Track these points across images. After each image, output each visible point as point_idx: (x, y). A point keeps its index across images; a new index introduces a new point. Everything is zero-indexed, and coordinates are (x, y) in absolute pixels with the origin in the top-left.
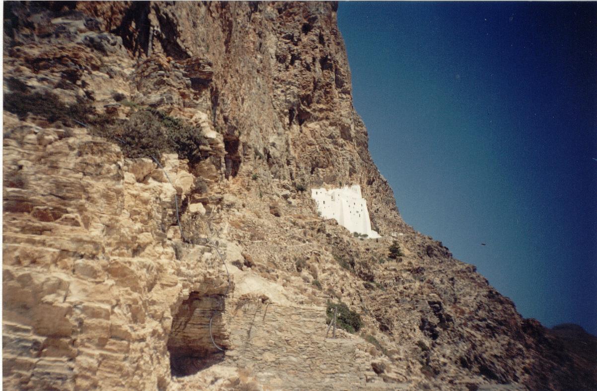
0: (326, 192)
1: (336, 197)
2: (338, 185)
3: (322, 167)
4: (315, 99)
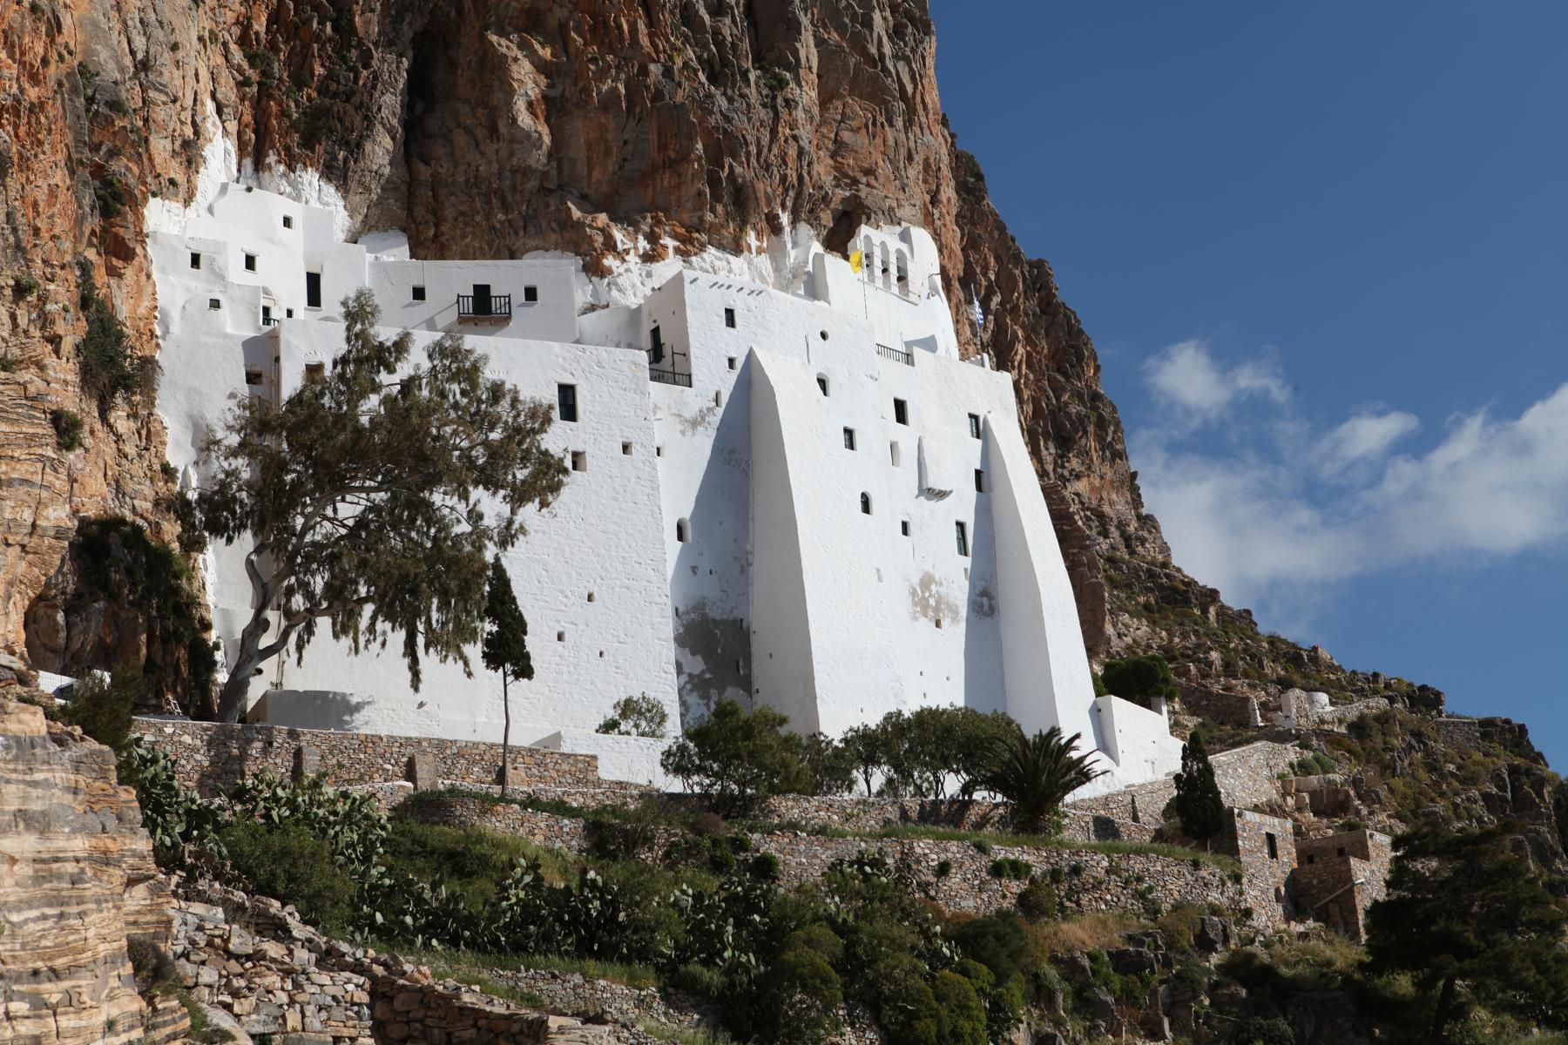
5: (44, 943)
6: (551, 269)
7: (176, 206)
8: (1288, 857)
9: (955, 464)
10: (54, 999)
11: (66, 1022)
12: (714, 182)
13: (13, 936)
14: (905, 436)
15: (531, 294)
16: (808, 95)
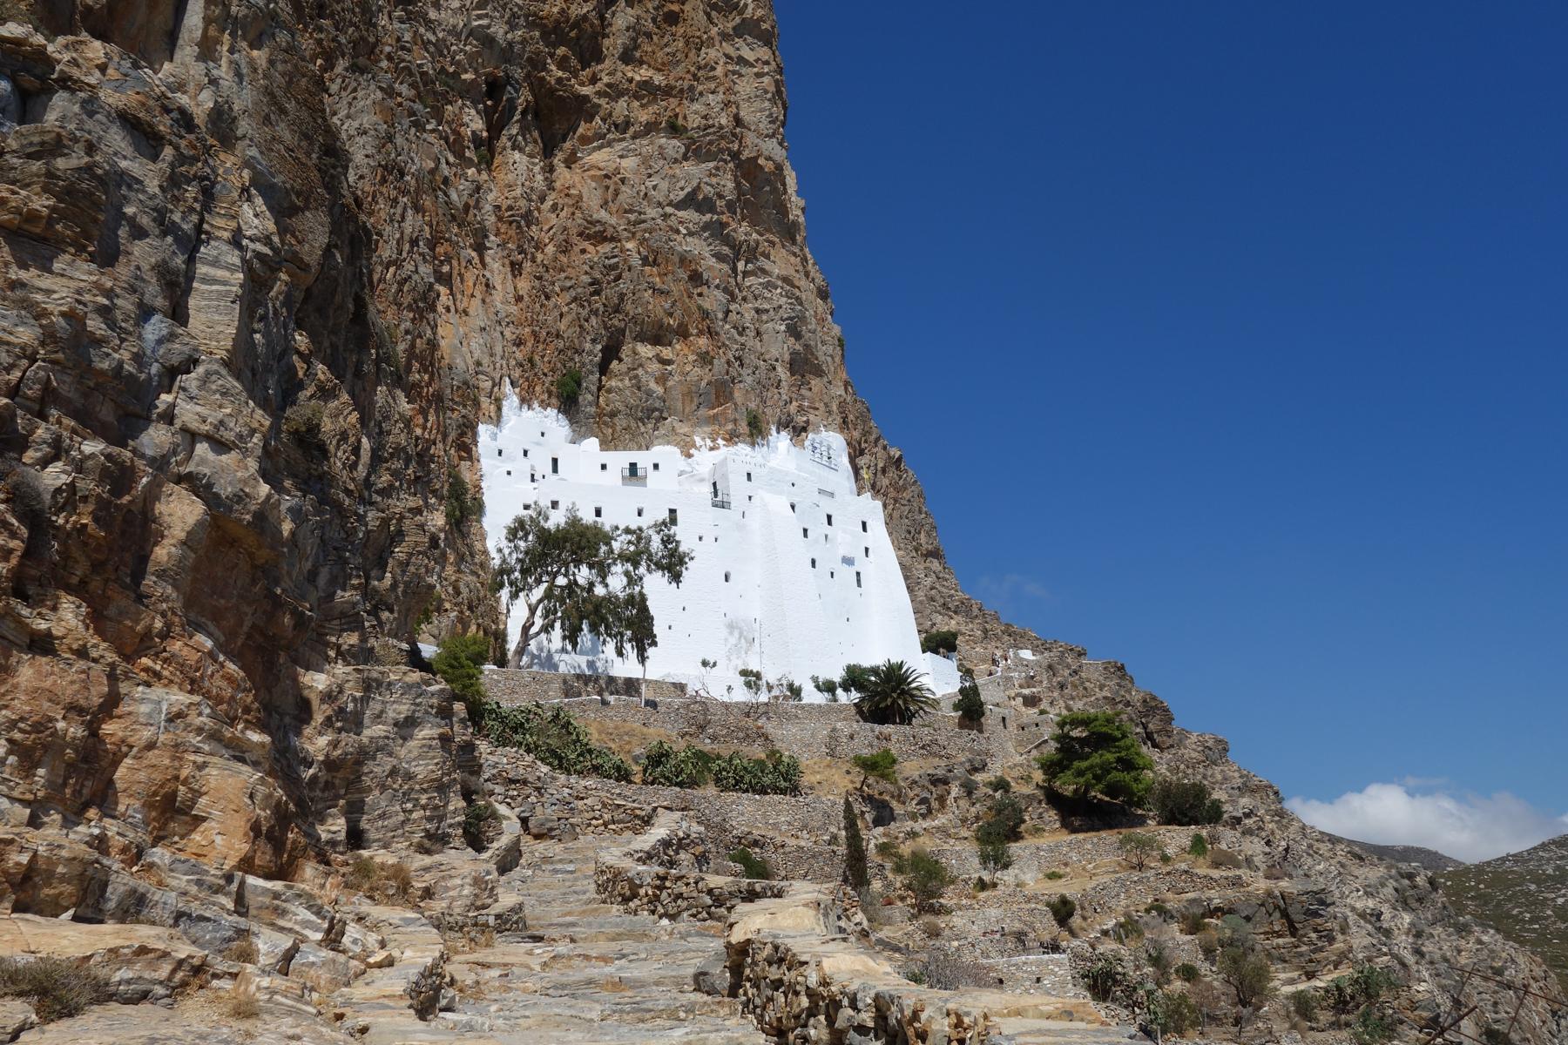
1: (736, 488)
2: (743, 428)
3: (656, 340)
4: (613, 44)
6: (664, 453)
7: (491, 427)
15: (656, 466)
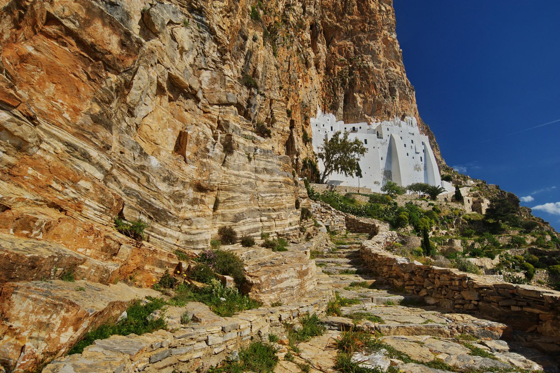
0: (368, 127)
1: (385, 134)
2: (386, 116)
5: (271, 202)
6: (364, 125)
7: (314, 118)
8: (471, 203)
9: (420, 149)
10: (274, 217)
11: (277, 223)
12: (385, 111)
13: (262, 200)
14: (413, 145)
15: (360, 128)
16: (397, 99)
